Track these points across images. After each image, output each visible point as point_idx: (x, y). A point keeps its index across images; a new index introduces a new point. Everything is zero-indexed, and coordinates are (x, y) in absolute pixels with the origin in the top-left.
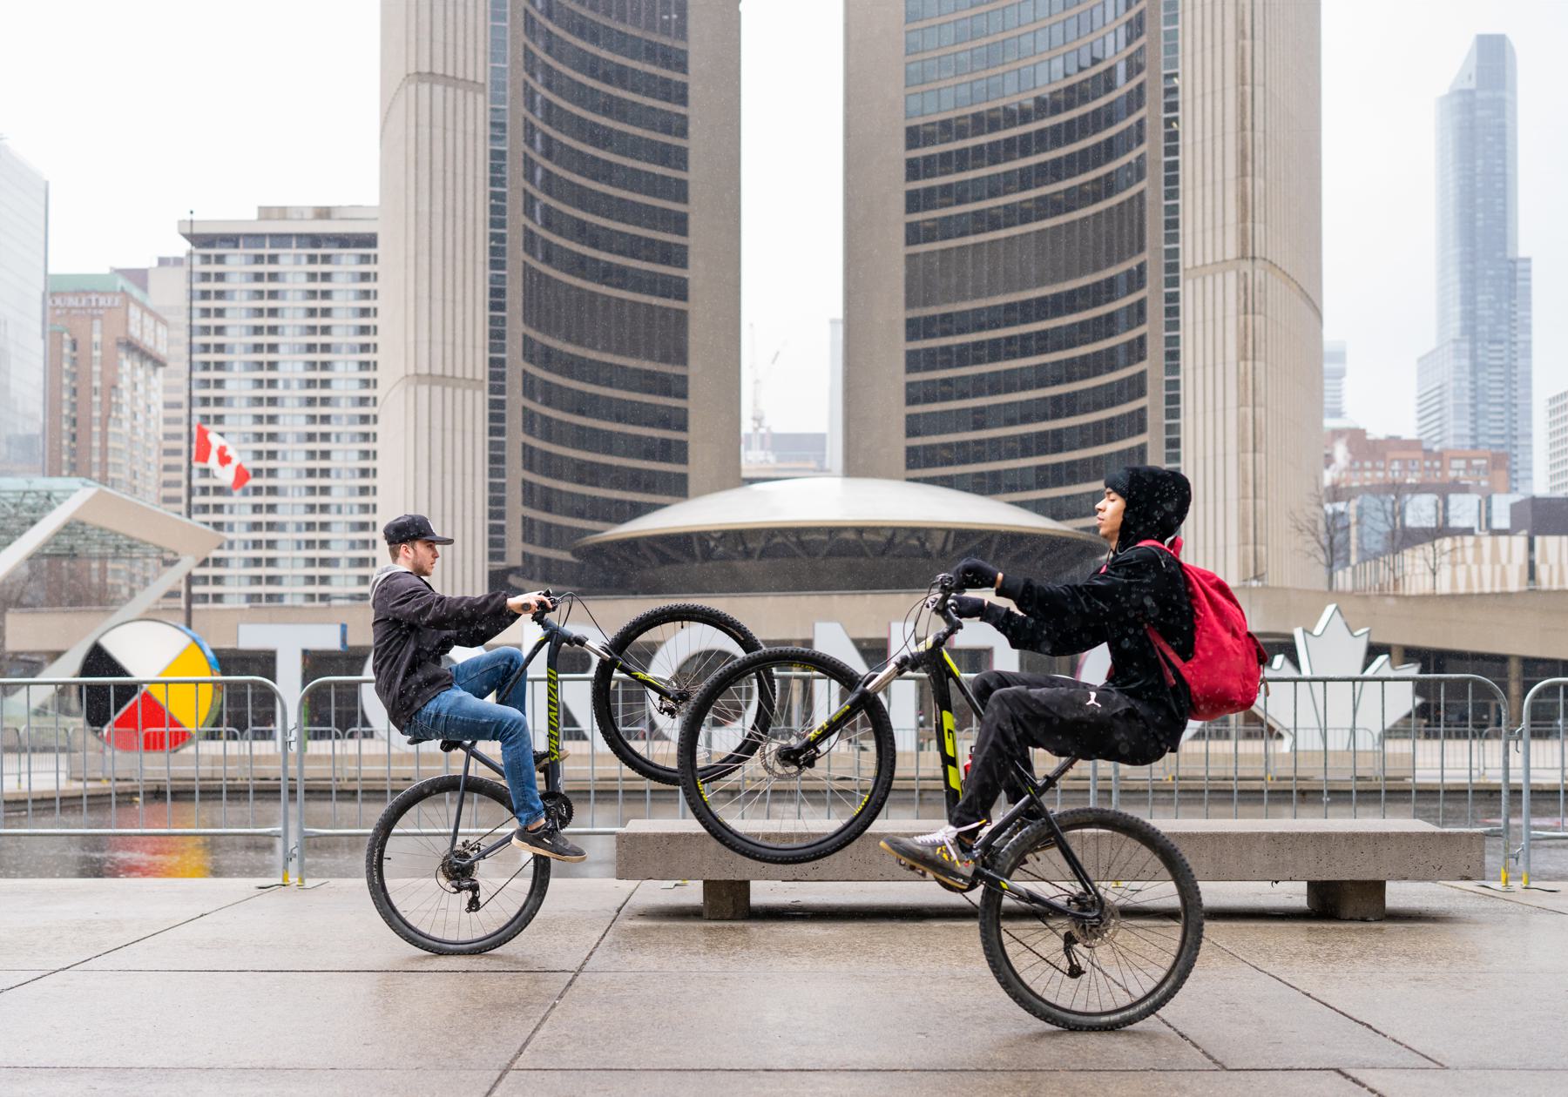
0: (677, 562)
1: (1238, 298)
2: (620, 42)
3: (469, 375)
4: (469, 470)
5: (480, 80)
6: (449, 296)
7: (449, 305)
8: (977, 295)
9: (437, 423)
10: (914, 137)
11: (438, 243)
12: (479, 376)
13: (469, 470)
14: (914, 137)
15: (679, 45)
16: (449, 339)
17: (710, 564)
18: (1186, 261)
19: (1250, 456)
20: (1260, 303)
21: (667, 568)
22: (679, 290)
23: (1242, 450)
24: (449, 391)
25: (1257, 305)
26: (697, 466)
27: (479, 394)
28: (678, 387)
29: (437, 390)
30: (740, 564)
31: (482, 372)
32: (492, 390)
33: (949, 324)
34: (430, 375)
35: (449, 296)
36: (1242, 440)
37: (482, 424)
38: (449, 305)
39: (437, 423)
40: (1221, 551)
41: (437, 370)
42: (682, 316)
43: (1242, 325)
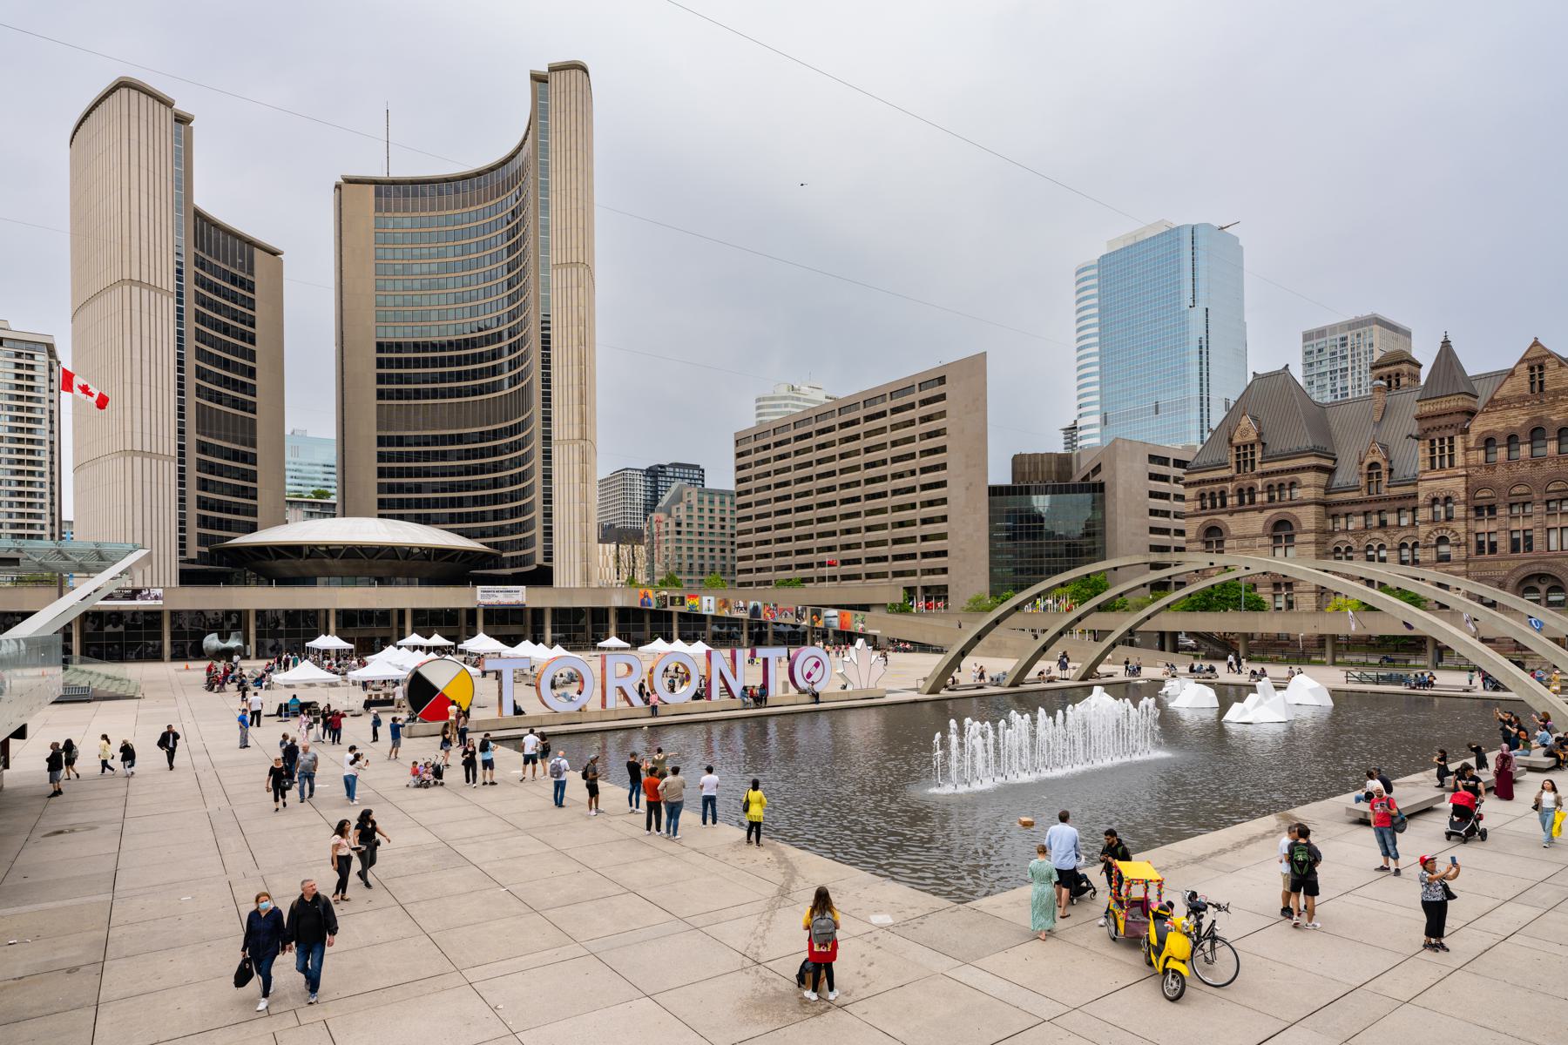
0: (289, 558)
2: (224, 275)
7: (153, 414)
8: (417, 429)
9: (147, 478)
10: (380, 347)
11: (146, 379)
12: (172, 454)
14: (380, 347)
15: (249, 278)
16: (154, 432)
17: (309, 560)
18: (555, 436)
21: (280, 561)
23: (581, 522)
24: (154, 461)
26: (264, 502)
27: (172, 464)
28: (251, 459)
30: (326, 560)
31: (174, 451)
32: (181, 462)
33: (400, 441)
36: (581, 517)
37: (174, 480)
39: (147, 478)
40: (572, 564)
41: (147, 449)
42: (253, 421)
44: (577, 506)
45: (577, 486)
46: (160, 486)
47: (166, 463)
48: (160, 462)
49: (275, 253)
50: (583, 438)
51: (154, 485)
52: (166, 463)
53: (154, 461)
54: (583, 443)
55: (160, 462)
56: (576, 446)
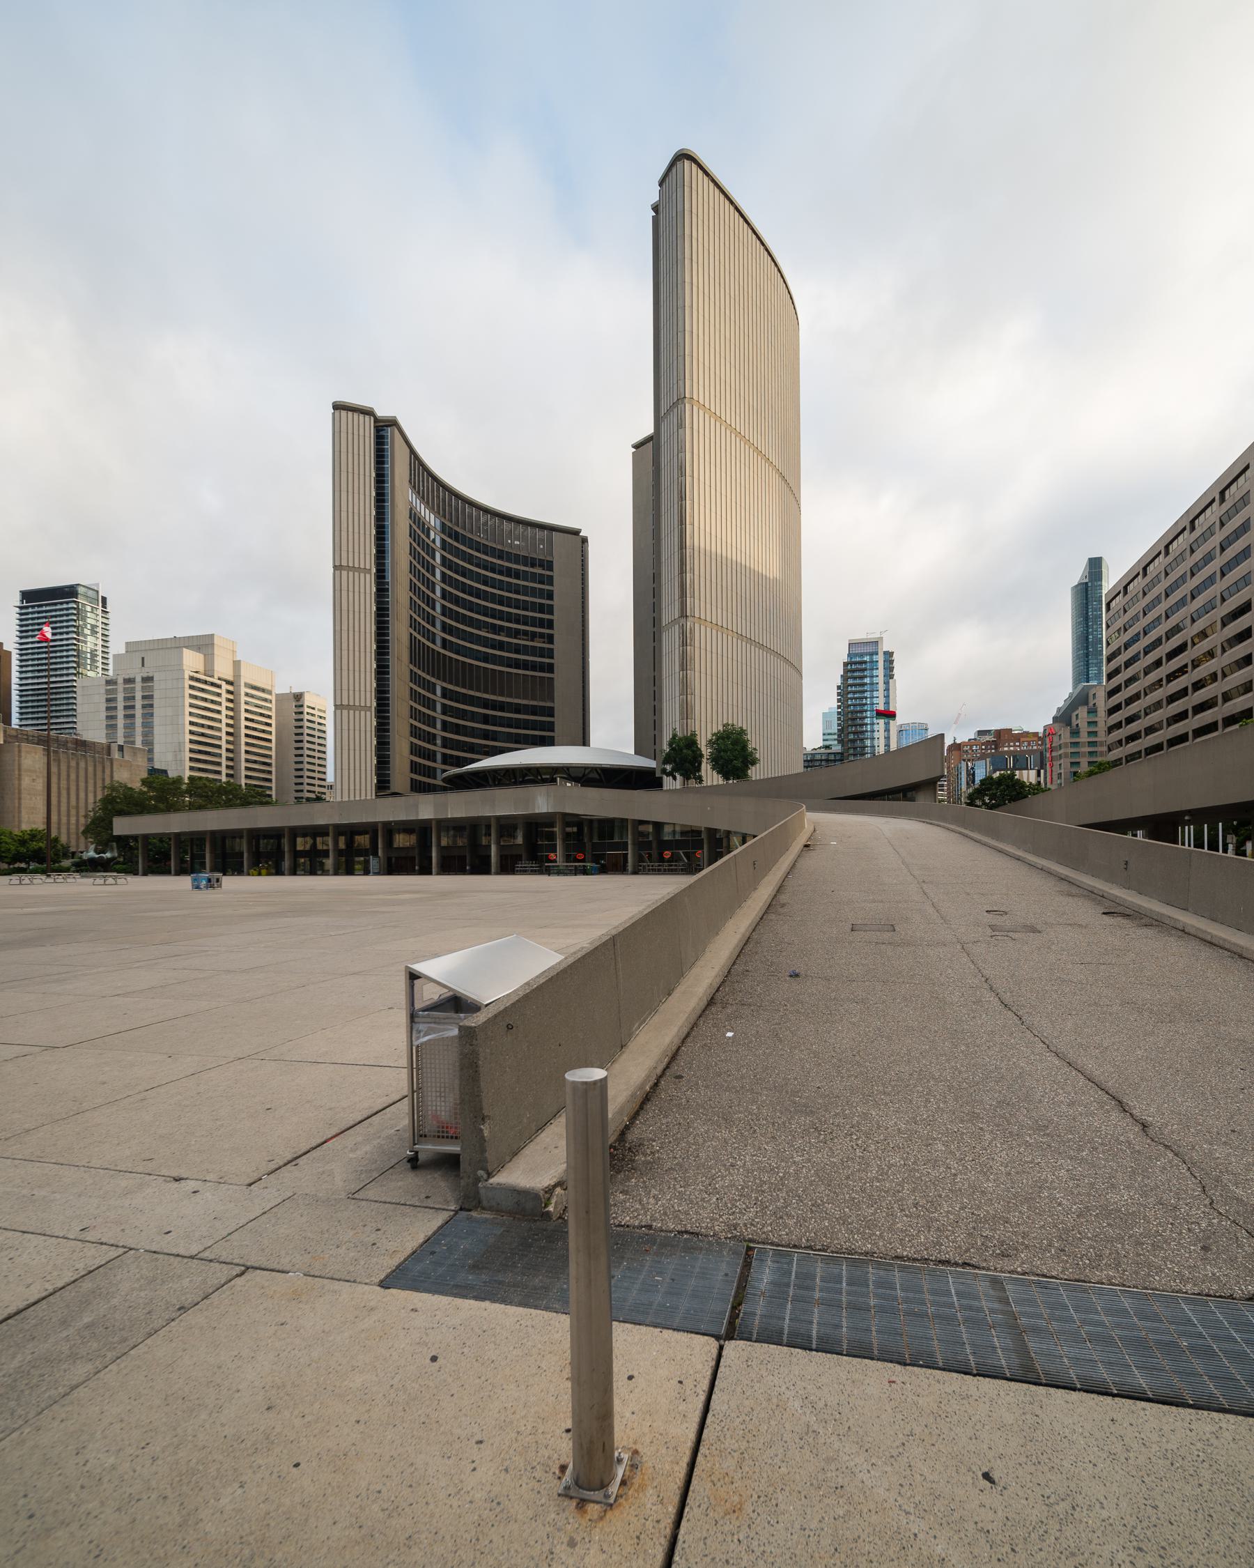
1: (679, 638)
3: (363, 704)
4: (363, 748)
5: (368, 567)
6: (351, 668)
7: (351, 673)
13: (363, 748)
15: (549, 558)
19: (685, 721)
20: (691, 640)
22: (550, 668)
24: (351, 712)
25: (688, 641)
27: (368, 713)
29: (345, 712)
34: (342, 705)
35: (351, 668)
36: (682, 713)
38: (351, 673)
41: (345, 703)
43: (681, 652)
44: (677, 698)
45: (677, 675)
46: (357, 733)
47: (363, 713)
48: (357, 712)
49: (576, 533)
50: (683, 615)
51: (352, 732)
52: (363, 713)
53: (351, 712)
54: (683, 621)
55: (357, 712)
56: (677, 626)
